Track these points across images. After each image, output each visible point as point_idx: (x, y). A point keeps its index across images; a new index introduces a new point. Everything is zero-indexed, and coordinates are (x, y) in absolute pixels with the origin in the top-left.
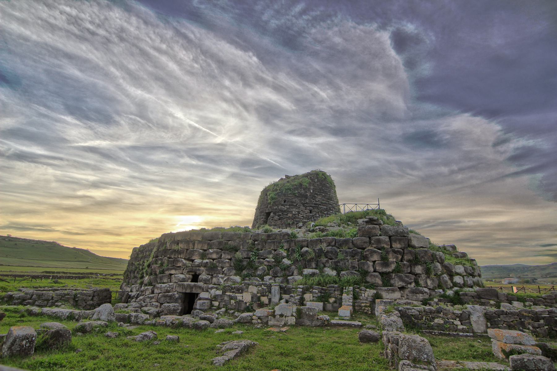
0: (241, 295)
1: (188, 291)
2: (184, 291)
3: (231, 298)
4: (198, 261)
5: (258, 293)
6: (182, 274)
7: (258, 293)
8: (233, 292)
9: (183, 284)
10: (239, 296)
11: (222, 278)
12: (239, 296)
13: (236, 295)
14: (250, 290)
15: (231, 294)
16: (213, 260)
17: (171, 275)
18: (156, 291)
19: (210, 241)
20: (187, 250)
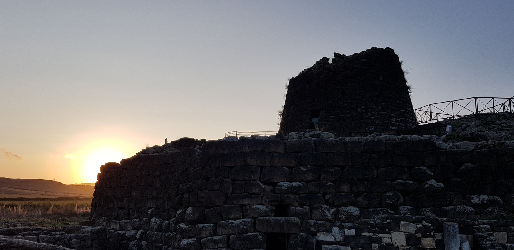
0: (389, 235)
1: (277, 230)
2: (270, 230)
3: (372, 240)
4: (285, 184)
5: (416, 233)
6: (262, 204)
7: (416, 233)
8: (374, 232)
9: (267, 220)
10: (386, 239)
11: (329, 210)
12: (386, 239)
13: (380, 235)
14: (402, 229)
15: (371, 234)
16: (307, 182)
17: (242, 205)
18: (220, 231)
19: (298, 153)
20: (262, 167)
